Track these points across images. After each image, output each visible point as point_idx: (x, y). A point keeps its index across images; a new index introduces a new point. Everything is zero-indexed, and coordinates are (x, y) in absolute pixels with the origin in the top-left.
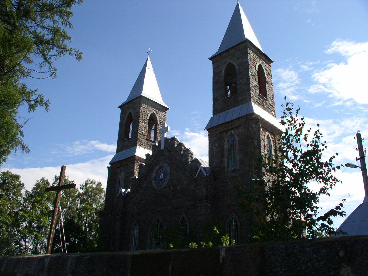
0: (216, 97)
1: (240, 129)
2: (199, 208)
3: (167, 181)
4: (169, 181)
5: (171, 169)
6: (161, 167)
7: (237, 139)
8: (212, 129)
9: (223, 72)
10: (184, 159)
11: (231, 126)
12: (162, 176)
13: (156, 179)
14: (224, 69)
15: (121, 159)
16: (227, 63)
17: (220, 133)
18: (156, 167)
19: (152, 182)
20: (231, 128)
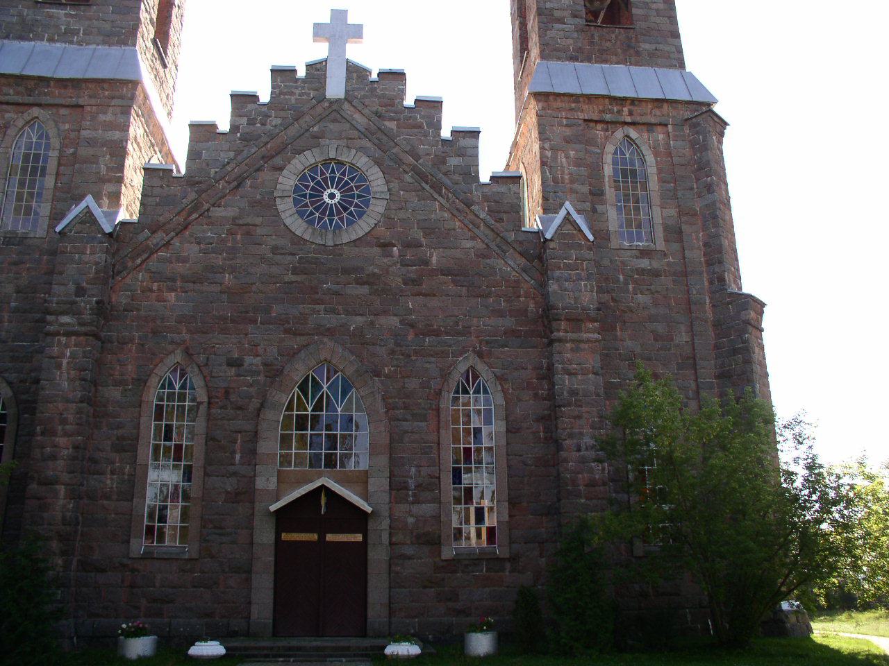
2: (568, 345)
3: (372, 222)
5: (387, 182)
8: (555, 99)
10: (453, 161)
11: (631, 113)
17: (585, 120)
20: (628, 119)
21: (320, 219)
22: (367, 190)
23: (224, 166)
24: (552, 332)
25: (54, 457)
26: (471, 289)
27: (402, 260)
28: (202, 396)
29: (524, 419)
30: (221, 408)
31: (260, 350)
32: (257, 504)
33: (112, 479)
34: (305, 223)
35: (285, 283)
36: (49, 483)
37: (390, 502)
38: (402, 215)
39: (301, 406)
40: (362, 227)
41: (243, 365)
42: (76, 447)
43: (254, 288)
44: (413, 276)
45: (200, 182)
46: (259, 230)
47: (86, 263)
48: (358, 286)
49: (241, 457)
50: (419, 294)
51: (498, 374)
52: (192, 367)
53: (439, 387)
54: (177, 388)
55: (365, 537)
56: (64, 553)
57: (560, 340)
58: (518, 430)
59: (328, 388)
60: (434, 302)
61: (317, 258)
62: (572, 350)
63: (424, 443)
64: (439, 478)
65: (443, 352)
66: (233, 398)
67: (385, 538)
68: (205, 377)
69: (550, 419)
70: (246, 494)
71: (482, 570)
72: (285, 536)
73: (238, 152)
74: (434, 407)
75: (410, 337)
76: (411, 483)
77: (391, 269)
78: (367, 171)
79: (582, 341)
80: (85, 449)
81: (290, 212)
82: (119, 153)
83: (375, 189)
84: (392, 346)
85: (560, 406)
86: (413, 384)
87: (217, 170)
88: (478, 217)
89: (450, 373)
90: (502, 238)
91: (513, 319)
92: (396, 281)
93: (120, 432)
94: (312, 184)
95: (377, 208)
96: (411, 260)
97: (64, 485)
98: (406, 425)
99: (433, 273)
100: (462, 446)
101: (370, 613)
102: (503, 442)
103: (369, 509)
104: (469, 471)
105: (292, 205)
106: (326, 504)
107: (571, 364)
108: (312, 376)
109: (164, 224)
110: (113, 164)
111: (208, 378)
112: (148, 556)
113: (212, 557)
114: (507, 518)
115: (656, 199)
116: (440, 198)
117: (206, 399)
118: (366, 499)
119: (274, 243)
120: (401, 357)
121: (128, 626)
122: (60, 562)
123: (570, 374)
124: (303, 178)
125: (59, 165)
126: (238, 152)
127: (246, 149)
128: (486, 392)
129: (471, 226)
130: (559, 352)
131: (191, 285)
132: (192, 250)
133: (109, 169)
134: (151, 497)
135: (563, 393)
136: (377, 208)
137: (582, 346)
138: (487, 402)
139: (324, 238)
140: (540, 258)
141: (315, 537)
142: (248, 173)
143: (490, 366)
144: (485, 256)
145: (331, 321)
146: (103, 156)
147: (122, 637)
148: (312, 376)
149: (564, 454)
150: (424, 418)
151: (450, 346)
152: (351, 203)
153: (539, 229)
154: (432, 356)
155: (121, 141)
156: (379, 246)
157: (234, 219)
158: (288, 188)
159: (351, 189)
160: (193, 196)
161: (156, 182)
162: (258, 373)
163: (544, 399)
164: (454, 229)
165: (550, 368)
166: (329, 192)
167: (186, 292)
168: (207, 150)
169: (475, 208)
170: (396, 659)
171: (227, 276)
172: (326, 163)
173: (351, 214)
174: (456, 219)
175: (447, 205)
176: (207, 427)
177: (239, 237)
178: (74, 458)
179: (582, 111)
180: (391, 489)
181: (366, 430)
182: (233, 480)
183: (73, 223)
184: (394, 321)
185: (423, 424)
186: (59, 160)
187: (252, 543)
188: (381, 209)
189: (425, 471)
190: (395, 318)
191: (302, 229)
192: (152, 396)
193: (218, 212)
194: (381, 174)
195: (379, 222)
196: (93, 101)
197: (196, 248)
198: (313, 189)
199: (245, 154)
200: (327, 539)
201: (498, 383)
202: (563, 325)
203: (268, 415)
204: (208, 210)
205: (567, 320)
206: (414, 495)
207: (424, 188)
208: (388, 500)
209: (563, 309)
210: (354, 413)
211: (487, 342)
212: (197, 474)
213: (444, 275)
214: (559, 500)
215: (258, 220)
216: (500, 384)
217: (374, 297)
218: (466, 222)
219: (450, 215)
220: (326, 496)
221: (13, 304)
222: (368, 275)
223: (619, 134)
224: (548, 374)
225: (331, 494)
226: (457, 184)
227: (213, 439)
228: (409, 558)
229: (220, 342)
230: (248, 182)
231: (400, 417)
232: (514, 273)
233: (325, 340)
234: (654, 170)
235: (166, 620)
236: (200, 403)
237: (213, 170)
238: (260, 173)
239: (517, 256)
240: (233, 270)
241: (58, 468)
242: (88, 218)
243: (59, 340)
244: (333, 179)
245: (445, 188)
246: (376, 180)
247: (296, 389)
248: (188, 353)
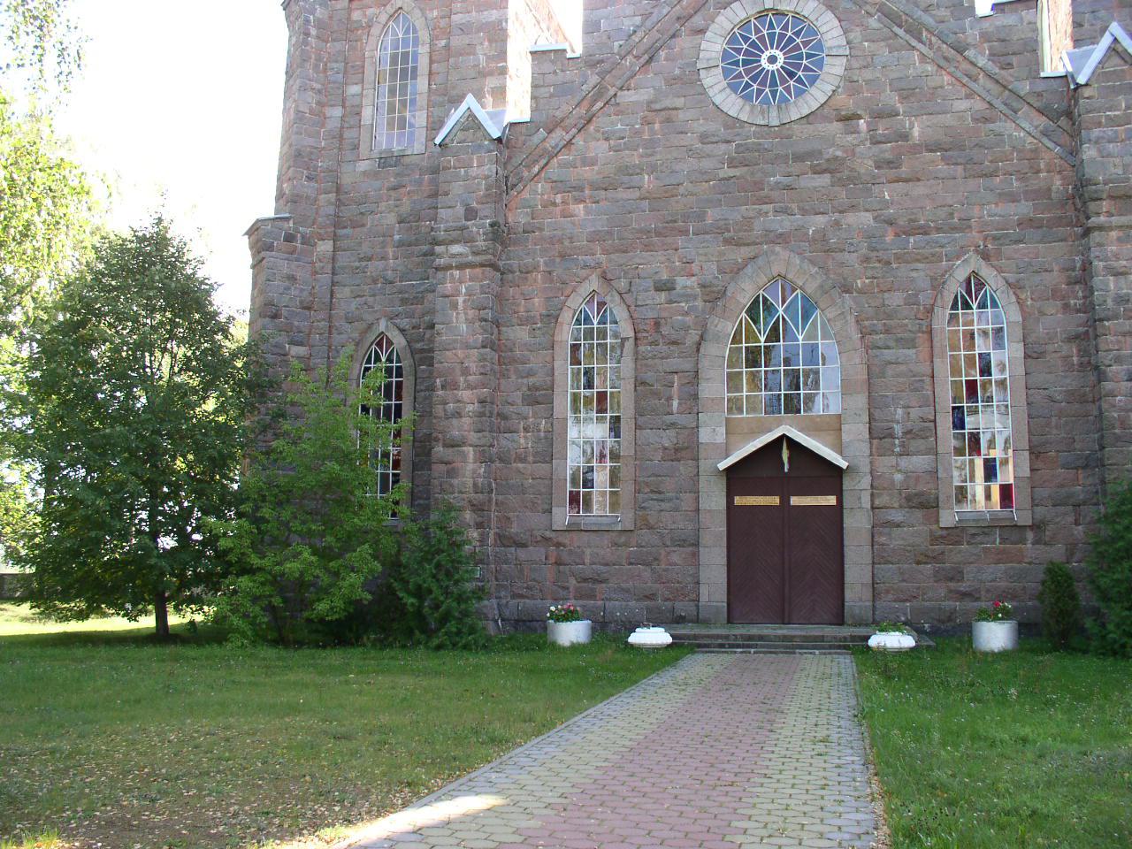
2: (1114, 234)
3: (829, 89)
21: (760, 92)
22: (819, 46)
23: (630, 36)
24: (1088, 218)
25: (458, 415)
26: (969, 166)
27: (871, 136)
28: (627, 330)
29: (1050, 339)
30: (651, 344)
31: (695, 267)
32: (702, 463)
33: (525, 437)
34: (740, 100)
36: (453, 444)
37: (871, 455)
38: (868, 74)
39: (751, 336)
40: (816, 96)
41: (674, 289)
42: (482, 402)
43: (681, 190)
44: (888, 156)
45: (602, 61)
46: (681, 115)
47: (475, 178)
48: (816, 176)
49: (680, 404)
51: (1010, 281)
52: (612, 296)
53: (932, 302)
54: (595, 322)
55: (840, 501)
56: (479, 525)
57: (1100, 228)
59: (785, 311)
60: (919, 190)
61: (760, 144)
62: (1119, 239)
63: (914, 376)
64: (935, 421)
65: (933, 255)
66: (665, 330)
67: (866, 501)
68: (629, 306)
69: (1087, 336)
70: (687, 449)
71: (994, 543)
72: (738, 501)
73: (646, 16)
74: (924, 329)
75: (889, 238)
76: (898, 429)
77: (858, 150)
78: (817, 19)
80: (492, 403)
81: (720, 87)
82: (498, 35)
83: (827, 44)
84: (864, 251)
85: (1101, 320)
86: (895, 299)
87: (621, 42)
88: (975, 65)
89: (944, 283)
90: (1010, 90)
91: (1031, 203)
92: (865, 165)
93: (531, 380)
94: (745, 47)
95: (834, 69)
96: (884, 135)
97: (471, 446)
98: (888, 354)
99: (915, 149)
101: (848, 595)
102: (1021, 371)
103: (843, 464)
104: (975, 412)
105: (721, 77)
106: (789, 458)
107: (1118, 259)
108: (763, 296)
110: (493, 53)
111: (633, 307)
112: (573, 529)
113: (650, 528)
114: (1027, 473)
116: (919, 46)
117: (632, 334)
118: (841, 453)
119: (702, 129)
120: (877, 265)
121: (557, 609)
122: (475, 535)
124: (733, 40)
125: (431, 62)
126: (646, 16)
127: (656, 10)
128: (994, 304)
129: (965, 80)
130: (1100, 245)
131: (603, 192)
132: (600, 149)
133: (489, 58)
134: (574, 459)
135: (1105, 301)
136: (834, 69)
138: (997, 318)
139: (766, 116)
140: (1069, 114)
141: (775, 501)
142: (660, 42)
143: (1000, 270)
144: (986, 120)
145: (784, 224)
146: (481, 44)
147: (551, 621)
148: (763, 296)
149: (1108, 385)
150: (911, 344)
151: (942, 247)
152: (798, 66)
153: (1067, 72)
154: (918, 261)
155: (500, 22)
156: (840, 120)
157: (650, 103)
158: (714, 55)
159: (797, 47)
160: (594, 79)
161: (548, 67)
162: (695, 297)
163: (1078, 311)
164: (942, 87)
165: (1087, 267)
167: (597, 202)
168: (607, 18)
169: (970, 53)
170: (883, 652)
171: (646, 177)
172: (761, 16)
173: (799, 81)
174: (944, 72)
175: (931, 54)
176: (636, 369)
177: (657, 126)
178: (481, 415)
180: (871, 437)
181: (836, 363)
182: (671, 433)
183: (454, 131)
184: (866, 219)
185: (912, 352)
186: (431, 57)
187: (698, 510)
188: (839, 70)
189: (915, 413)
190: (867, 214)
191: (737, 107)
192: (566, 333)
193: (627, 97)
194: (836, 22)
195: (838, 87)
197: (605, 145)
198: (747, 53)
199: (654, 18)
200: (792, 503)
201: (1011, 293)
202: (1105, 205)
203: (709, 349)
204: (615, 94)
205: (1112, 197)
206: (902, 445)
207: (896, 35)
208: (868, 452)
209: (1105, 185)
210: (820, 342)
211: (995, 238)
212: (626, 427)
213: (931, 151)
214: (1102, 448)
215: (680, 102)
216: (1014, 293)
217: (836, 188)
218: (959, 74)
219: (935, 68)
220: (788, 448)
221: (397, 237)
222: (828, 160)
224: (1083, 276)
225: (794, 446)
226: (943, 22)
227: (643, 383)
228: (898, 526)
229: (642, 261)
230: (662, 54)
231: (880, 344)
232: (1030, 139)
233: (777, 249)
235: (600, 603)
236: (624, 340)
237: (616, 44)
238: (679, 39)
239: (1034, 114)
240: (653, 169)
241: (462, 427)
242: (472, 123)
243: (452, 275)
244: (771, 36)
245: (927, 30)
246: (830, 30)
247: (744, 314)
248: (604, 278)
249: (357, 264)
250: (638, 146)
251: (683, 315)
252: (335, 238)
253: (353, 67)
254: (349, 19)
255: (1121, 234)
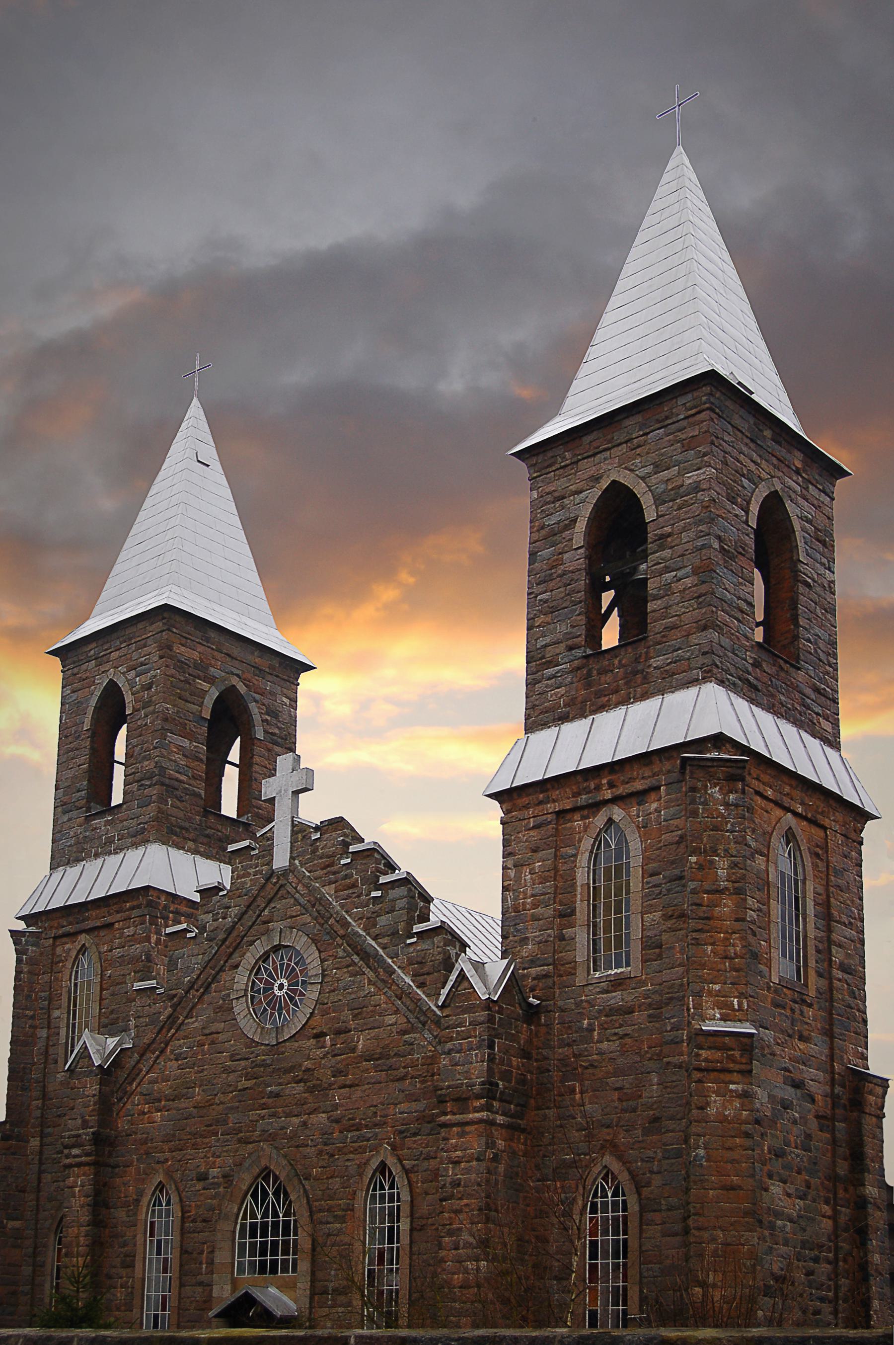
0: (546, 646)
1: (654, 805)
4: (314, 1010)
6: (276, 949)
7: (635, 845)
9: (581, 526)
12: (281, 988)
13: (253, 997)
14: (586, 511)
15: (78, 898)
16: (605, 483)
18: (252, 943)
19: (236, 1010)
20: (608, 795)
29: (429, 1214)
33: (121, 1293)
35: (240, 1090)
38: (334, 997)
41: (208, 1179)
46: (221, 1037)
47: (88, 1096)
49: (206, 1267)
50: (344, 1086)
58: (422, 1228)
60: (358, 1093)
79: (467, 1124)
100: (599, 1238)
109: (149, 1045)
115: (636, 904)
123: (452, 1163)
125: (102, 990)
132: (172, 1067)
137: (468, 1129)
145: (274, 1124)
166: (279, 983)
179: (554, 801)
183: (77, 1059)
186: (101, 986)
188: (315, 996)
190: (323, 1115)
194: (317, 954)
196: (118, 916)
205: (453, 1100)
211: (401, 1132)
223: (600, 820)
227: (186, 1252)
229: (192, 1157)
231: (324, 1220)
234: (640, 859)
249: (55, 1156)
250: (194, 1064)
251: (211, 1199)
252: (42, 1136)
253: (56, 994)
254: (53, 954)
255: (459, 1129)
